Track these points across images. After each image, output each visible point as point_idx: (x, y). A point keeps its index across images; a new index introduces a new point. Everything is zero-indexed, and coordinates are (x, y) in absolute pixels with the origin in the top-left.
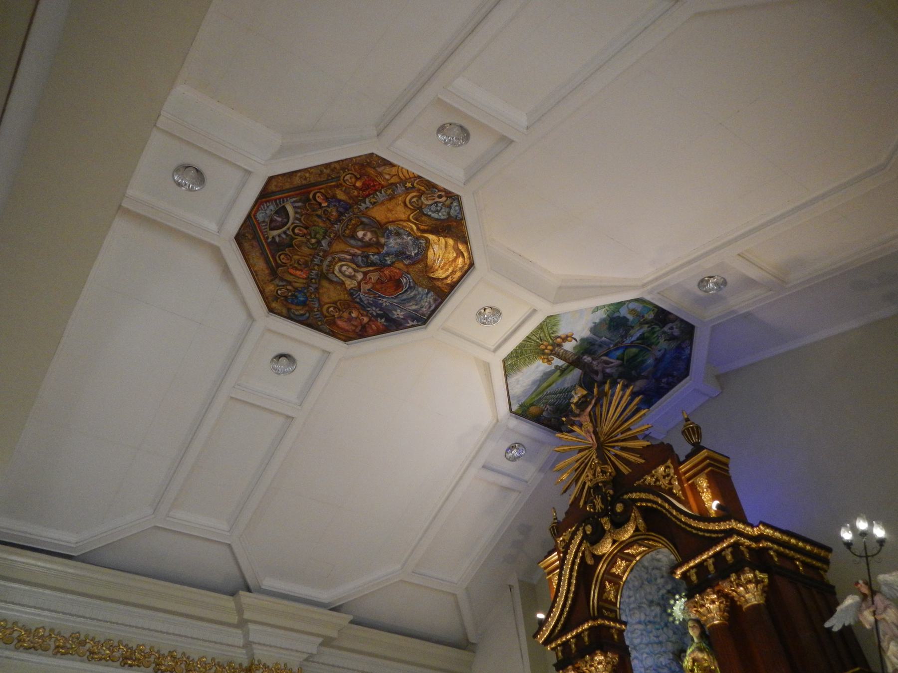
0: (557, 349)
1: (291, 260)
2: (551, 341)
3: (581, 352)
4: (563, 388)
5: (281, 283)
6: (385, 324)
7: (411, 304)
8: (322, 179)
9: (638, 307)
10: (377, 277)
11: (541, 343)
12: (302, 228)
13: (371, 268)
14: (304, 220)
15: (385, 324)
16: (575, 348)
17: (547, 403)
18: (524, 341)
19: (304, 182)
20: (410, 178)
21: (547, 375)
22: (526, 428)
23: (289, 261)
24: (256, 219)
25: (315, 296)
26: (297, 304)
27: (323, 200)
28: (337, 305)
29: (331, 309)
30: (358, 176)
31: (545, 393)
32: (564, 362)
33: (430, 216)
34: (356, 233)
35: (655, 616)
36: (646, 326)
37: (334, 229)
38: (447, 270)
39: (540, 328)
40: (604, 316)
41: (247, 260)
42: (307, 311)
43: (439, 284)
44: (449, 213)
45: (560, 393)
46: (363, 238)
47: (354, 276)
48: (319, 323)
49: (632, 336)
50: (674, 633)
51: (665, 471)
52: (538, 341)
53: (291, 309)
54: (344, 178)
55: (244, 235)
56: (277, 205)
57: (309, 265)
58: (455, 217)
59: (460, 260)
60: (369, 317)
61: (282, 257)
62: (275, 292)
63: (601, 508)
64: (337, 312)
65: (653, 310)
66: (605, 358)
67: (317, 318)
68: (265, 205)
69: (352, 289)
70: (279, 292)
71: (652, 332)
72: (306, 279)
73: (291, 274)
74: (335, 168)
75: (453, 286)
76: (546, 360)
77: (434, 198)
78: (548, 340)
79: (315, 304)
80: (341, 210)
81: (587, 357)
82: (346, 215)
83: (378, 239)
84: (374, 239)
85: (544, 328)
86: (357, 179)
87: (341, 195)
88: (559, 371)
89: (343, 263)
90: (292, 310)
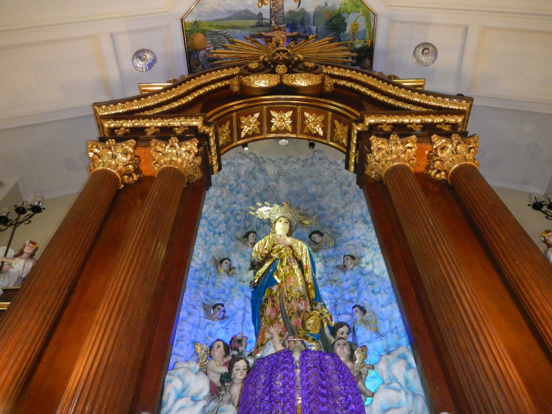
3: (290, 22)
9: (362, 26)
16: (291, 12)
17: (215, 43)
31: (225, 32)
32: (269, 18)
35: (215, 220)
40: (338, 7)
50: (223, 244)
65: (365, 42)
88: (257, 21)
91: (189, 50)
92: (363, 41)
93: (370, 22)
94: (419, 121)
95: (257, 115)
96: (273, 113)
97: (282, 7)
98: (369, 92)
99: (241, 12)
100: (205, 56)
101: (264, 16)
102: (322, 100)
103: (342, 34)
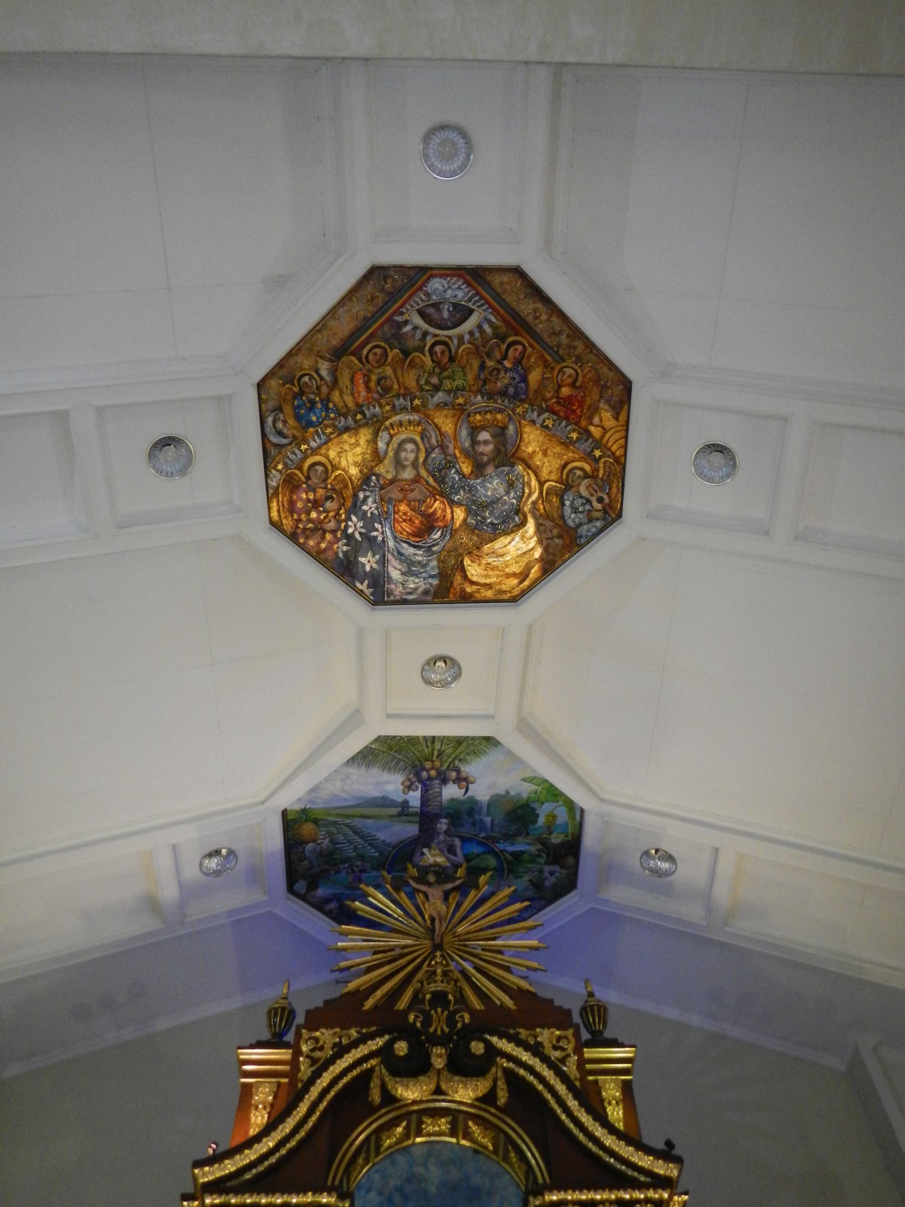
0: (437, 781)
1: (378, 367)
2: (445, 767)
3: (450, 811)
4: (374, 833)
5: (324, 373)
6: (341, 555)
7: (399, 567)
8: (548, 341)
10: (419, 497)
11: (434, 758)
12: (447, 354)
13: (431, 480)
14: (464, 350)
15: (341, 555)
16: (452, 800)
18: (425, 738)
19: (530, 318)
20: (609, 449)
21: (385, 802)
22: (275, 841)
23: (375, 364)
24: (427, 280)
25: (331, 433)
26: (298, 417)
27: (515, 358)
28: (333, 471)
29: (320, 468)
30: (578, 384)
33: (563, 504)
36: (539, 846)
38: (487, 576)
39: (459, 741)
40: (525, 795)
41: (341, 303)
42: (294, 437)
43: (458, 579)
44: (580, 525)
45: (362, 837)
46: (479, 443)
47: (404, 467)
48: (280, 467)
49: (512, 844)
51: (559, 1039)
52: (436, 753)
53: (282, 412)
55: (386, 278)
56: (470, 300)
57: (386, 396)
58: (578, 535)
59: (514, 581)
60: (340, 526)
61: (378, 350)
62: (301, 373)
63: (442, 1030)
64: (319, 480)
65: (567, 836)
66: (457, 842)
69: (378, 476)
70: (306, 379)
71: (533, 859)
72: (358, 405)
73: (352, 380)
74: (575, 348)
75: (466, 599)
76: (408, 783)
77: (594, 493)
78: (445, 762)
79: (315, 441)
80: (511, 390)
81: (445, 823)
82: (506, 401)
83: (487, 463)
85: (464, 744)
86: (573, 385)
87: (534, 377)
88: (400, 809)
89: (418, 439)
90: (281, 416)
91: (290, 842)
92: (564, 835)
93: (575, 814)
94: (613, 1197)
95: (404, 1124)
96: (424, 1119)
97: (439, 794)
98: (556, 1107)
99: (376, 799)
100: (315, 849)
101: (411, 804)
102: (493, 1110)
103: (531, 827)
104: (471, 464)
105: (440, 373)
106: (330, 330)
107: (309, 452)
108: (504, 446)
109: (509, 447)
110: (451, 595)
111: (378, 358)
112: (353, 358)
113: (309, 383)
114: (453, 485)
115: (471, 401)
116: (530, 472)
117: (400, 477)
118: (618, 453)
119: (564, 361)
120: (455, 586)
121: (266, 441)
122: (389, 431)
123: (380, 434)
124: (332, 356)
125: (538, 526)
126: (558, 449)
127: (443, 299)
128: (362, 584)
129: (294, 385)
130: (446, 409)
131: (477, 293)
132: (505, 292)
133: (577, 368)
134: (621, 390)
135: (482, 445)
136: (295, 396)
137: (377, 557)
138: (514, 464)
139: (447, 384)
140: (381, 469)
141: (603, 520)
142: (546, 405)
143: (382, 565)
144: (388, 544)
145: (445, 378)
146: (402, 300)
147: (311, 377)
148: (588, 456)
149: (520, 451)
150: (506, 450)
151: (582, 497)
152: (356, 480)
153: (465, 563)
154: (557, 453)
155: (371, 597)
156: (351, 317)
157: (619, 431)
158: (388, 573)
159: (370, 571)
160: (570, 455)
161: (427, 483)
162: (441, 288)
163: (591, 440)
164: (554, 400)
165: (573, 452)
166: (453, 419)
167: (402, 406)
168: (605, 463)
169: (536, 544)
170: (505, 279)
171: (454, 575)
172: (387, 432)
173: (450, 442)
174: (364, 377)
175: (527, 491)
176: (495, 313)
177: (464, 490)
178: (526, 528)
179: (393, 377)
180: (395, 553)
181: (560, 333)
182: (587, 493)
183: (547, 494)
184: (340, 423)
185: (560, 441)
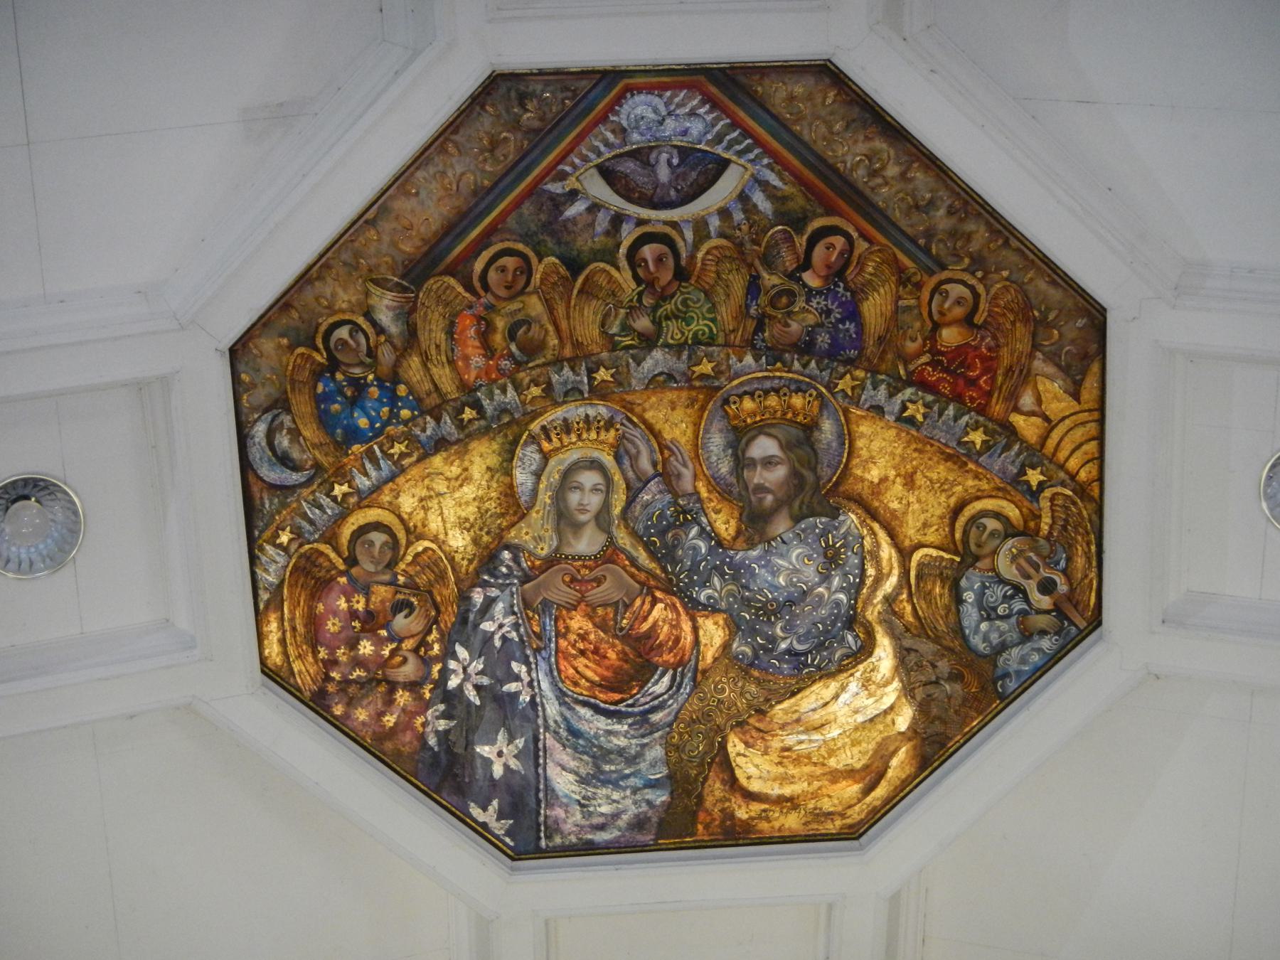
1: (511, 298)
5: (385, 318)
6: (432, 741)
7: (573, 764)
8: (903, 224)
10: (616, 596)
12: (670, 262)
13: (642, 557)
14: (708, 253)
15: (432, 741)
19: (860, 175)
20: (1062, 467)
23: (502, 293)
24: (619, 100)
25: (403, 455)
26: (325, 421)
27: (828, 267)
28: (409, 544)
29: (378, 538)
30: (979, 319)
33: (959, 600)
34: (760, 433)
37: (733, 360)
38: (785, 779)
41: (421, 159)
42: (318, 467)
43: (715, 788)
44: (1003, 647)
46: (753, 463)
47: (577, 527)
48: (284, 538)
53: (288, 410)
54: (949, 281)
55: (522, 99)
56: (718, 139)
57: (531, 365)
58: (999, 672)
59: (851, 789)
60: (429, 673)
61: (510, 262)
62: (331, 320)
64: (377, 563)
67: (304, 516)
68: (695, 102)
69: (515, 550)
70: (343, 333)
72: (465, 387)
73: (450, 332)
74: (969, 237)
77: (1032, 571)
79: (366, 474)
80: (823, 340)
82: (813, 364)
83: (775, 510)
84: (770, 498)
86: (968, 321)
87: (875, 308)
89: (608, 460)
90: (287, 420)
104: (736, 514)
105: (655, 308)
106: (397, 218)
107: (353, 500)
108: (814, 470)
109: (825, 472)
110: (700, 827)
111: (510, 278)
112: (452, 281)
113: (351, 342)
114: (696, 564)
115: (729, 367)
116: (876, 526)
117: (568, 551)
118: (1083, 475)
119: (943, 267)
120: (708, 803)
121: (252, 479)
122: (539, 445)
123: (519, 452)
124: (403, 277)
125: (903, 655)
126: (941, 471)
127: (657, 140)
128: (485, 809)
129: (317, 350)
130: (672, 389)
131: (735, 124)
132: (800, 118)
133: (972, 281)
134: (1080, 329)
135: (759, 468)
136: (318, 373)
137: (520, 742)
138: (838, 509)
139: (673, 332)
140: (522, 535)
141: (1056, 634)
142: (906, 370)
143: (531, 763)
144: (544, 710)
145: (667, 318)
146: (563, 145)
147: (356, 328)
148: (1015, 484)
149: (851, 480)
150: (818, 478)
151: (1002, 581)
152: (465, 563)
153: (730, 748)
154: (938, 481)
155: (508, 840)
156: (446, 189)
157: (1083, 424)
158: (546, 778)
159: (504, 776)
160: (970, 483)
161: (633, 562)
162: (652, 116)
163: (1016, 447)
164: (925, 359)
165: (977, 477)
166: (689, 411)
167: (569, 387)
168: (1052, 499)
169: (898, 698)
170: (799, 90)
171: (706, 779)
172: (534, 447)
173: (685, 465)
174: (479, 324)
175: (871, 571)
176: (778, 168)
177: (722, 574)
178: (873, 659)
179: (545, 319)
180: (564, 733)
181: (931, 203)
182: (1016, 572)
183: (919, 577)
184: (424, 430)
185: (943, 453)
